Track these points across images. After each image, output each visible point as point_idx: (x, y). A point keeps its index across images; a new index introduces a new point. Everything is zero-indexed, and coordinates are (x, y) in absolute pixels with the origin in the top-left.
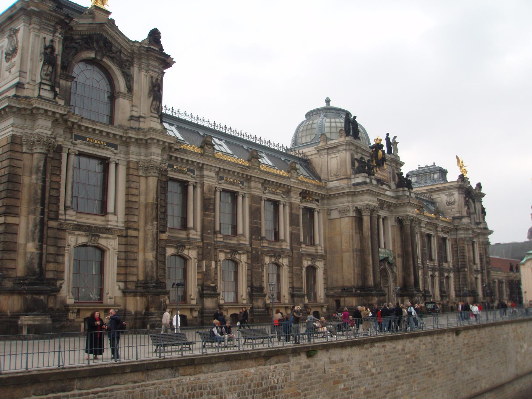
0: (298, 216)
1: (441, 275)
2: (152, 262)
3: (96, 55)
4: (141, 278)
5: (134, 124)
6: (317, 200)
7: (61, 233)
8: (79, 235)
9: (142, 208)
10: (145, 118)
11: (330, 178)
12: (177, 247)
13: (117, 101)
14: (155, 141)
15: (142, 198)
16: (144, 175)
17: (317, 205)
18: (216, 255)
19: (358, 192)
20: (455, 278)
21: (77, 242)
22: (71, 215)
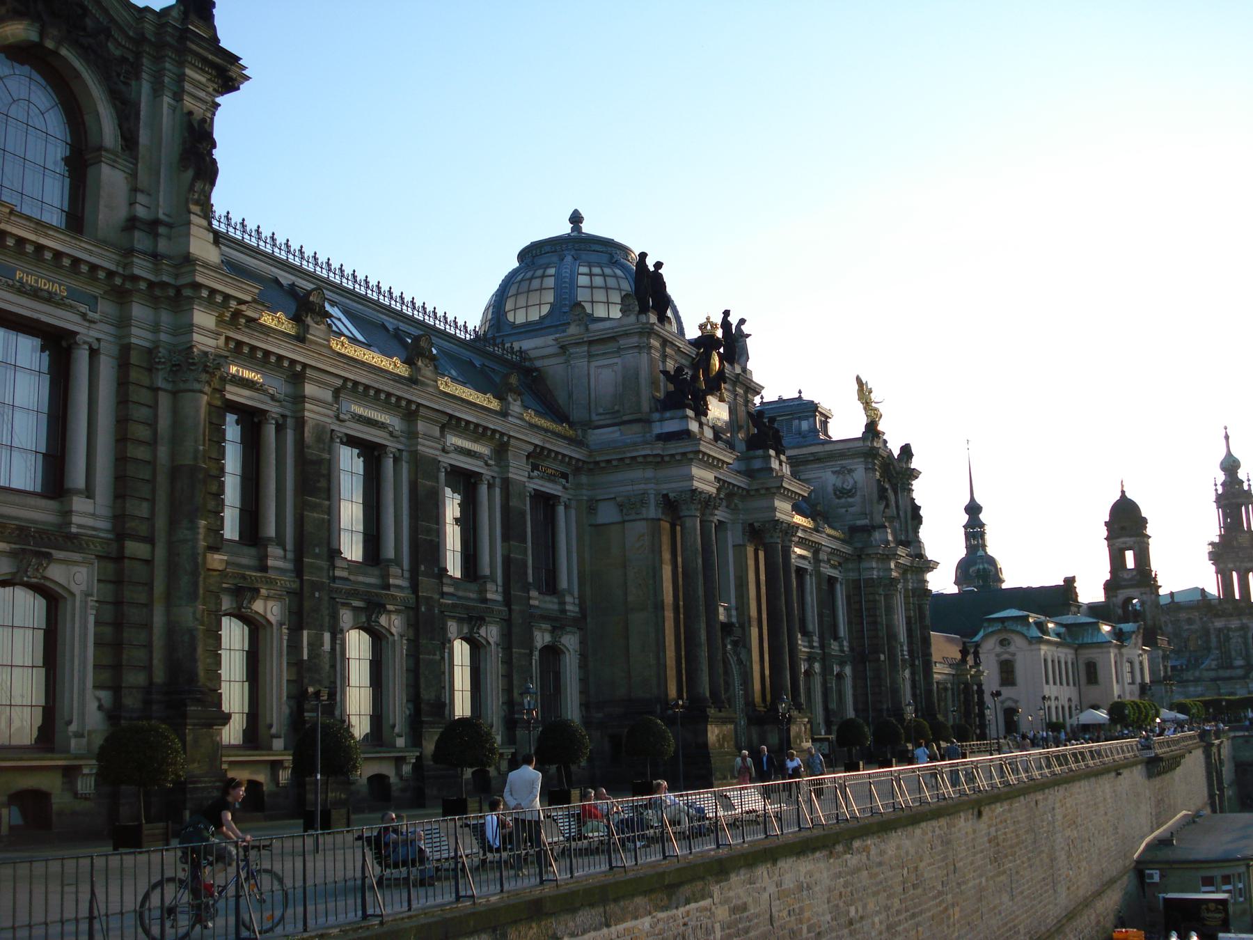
0: (523, 514)
1: (826, 670)
3: (42, 34)
4: (159, 676)
5: (140, 240)
6: (565, 476)
9: (162, 480)
10: (170, 226)
11: (594, 417)
13: (91, 171)
14: (205, 294)
15: (163, 452)
16: (169, 387)
17: (564, 487)
18: (335, 617)
19: (672, 456)
20: (854, 678)
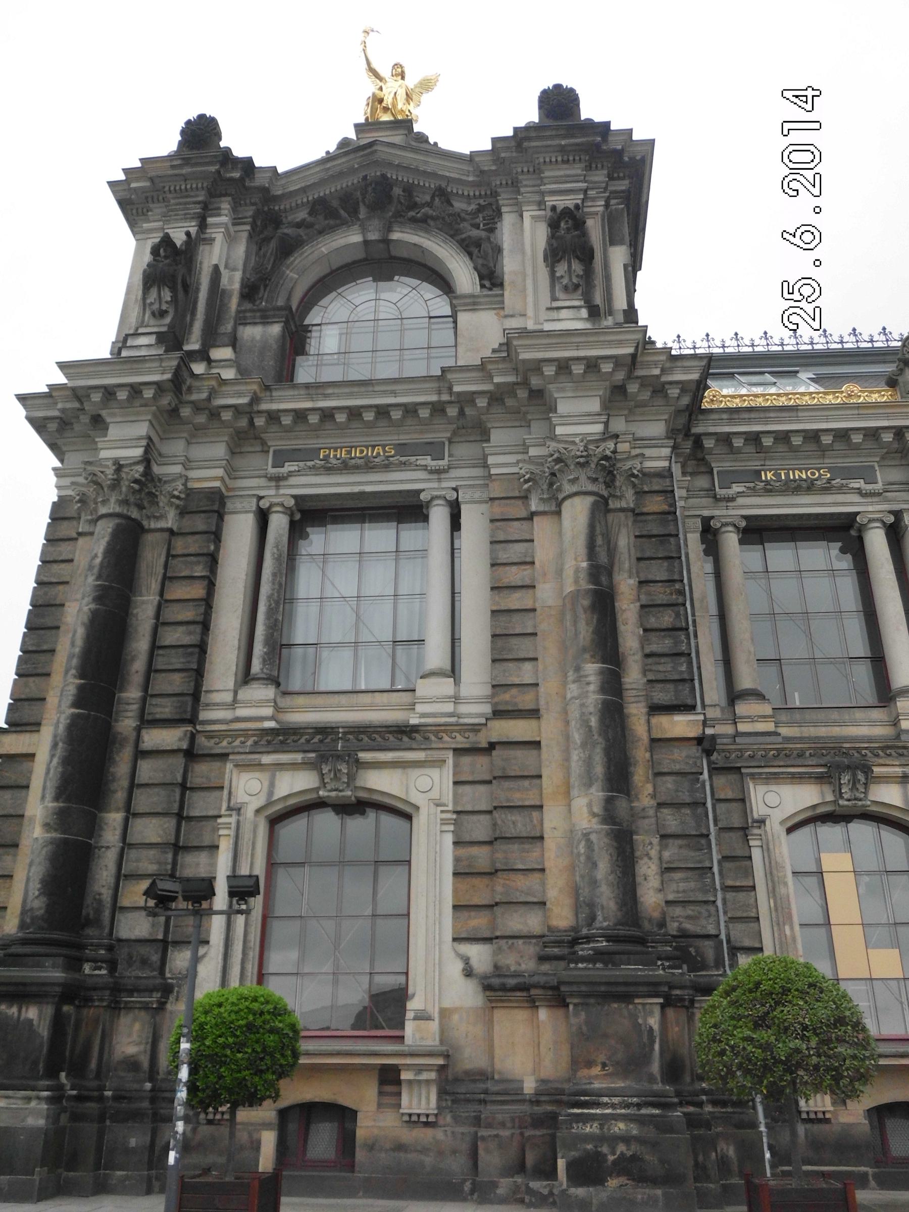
2: (586, 835)
7: (202, 771)
8: (280, 766)
12: (826, 778)
21: (271, 793)
22: (258, 705)
